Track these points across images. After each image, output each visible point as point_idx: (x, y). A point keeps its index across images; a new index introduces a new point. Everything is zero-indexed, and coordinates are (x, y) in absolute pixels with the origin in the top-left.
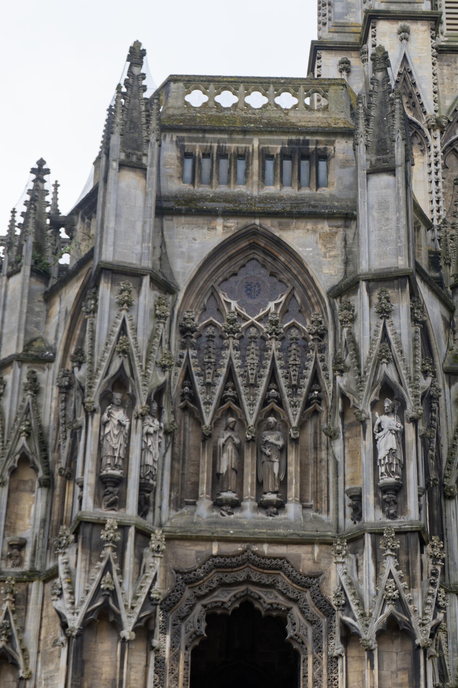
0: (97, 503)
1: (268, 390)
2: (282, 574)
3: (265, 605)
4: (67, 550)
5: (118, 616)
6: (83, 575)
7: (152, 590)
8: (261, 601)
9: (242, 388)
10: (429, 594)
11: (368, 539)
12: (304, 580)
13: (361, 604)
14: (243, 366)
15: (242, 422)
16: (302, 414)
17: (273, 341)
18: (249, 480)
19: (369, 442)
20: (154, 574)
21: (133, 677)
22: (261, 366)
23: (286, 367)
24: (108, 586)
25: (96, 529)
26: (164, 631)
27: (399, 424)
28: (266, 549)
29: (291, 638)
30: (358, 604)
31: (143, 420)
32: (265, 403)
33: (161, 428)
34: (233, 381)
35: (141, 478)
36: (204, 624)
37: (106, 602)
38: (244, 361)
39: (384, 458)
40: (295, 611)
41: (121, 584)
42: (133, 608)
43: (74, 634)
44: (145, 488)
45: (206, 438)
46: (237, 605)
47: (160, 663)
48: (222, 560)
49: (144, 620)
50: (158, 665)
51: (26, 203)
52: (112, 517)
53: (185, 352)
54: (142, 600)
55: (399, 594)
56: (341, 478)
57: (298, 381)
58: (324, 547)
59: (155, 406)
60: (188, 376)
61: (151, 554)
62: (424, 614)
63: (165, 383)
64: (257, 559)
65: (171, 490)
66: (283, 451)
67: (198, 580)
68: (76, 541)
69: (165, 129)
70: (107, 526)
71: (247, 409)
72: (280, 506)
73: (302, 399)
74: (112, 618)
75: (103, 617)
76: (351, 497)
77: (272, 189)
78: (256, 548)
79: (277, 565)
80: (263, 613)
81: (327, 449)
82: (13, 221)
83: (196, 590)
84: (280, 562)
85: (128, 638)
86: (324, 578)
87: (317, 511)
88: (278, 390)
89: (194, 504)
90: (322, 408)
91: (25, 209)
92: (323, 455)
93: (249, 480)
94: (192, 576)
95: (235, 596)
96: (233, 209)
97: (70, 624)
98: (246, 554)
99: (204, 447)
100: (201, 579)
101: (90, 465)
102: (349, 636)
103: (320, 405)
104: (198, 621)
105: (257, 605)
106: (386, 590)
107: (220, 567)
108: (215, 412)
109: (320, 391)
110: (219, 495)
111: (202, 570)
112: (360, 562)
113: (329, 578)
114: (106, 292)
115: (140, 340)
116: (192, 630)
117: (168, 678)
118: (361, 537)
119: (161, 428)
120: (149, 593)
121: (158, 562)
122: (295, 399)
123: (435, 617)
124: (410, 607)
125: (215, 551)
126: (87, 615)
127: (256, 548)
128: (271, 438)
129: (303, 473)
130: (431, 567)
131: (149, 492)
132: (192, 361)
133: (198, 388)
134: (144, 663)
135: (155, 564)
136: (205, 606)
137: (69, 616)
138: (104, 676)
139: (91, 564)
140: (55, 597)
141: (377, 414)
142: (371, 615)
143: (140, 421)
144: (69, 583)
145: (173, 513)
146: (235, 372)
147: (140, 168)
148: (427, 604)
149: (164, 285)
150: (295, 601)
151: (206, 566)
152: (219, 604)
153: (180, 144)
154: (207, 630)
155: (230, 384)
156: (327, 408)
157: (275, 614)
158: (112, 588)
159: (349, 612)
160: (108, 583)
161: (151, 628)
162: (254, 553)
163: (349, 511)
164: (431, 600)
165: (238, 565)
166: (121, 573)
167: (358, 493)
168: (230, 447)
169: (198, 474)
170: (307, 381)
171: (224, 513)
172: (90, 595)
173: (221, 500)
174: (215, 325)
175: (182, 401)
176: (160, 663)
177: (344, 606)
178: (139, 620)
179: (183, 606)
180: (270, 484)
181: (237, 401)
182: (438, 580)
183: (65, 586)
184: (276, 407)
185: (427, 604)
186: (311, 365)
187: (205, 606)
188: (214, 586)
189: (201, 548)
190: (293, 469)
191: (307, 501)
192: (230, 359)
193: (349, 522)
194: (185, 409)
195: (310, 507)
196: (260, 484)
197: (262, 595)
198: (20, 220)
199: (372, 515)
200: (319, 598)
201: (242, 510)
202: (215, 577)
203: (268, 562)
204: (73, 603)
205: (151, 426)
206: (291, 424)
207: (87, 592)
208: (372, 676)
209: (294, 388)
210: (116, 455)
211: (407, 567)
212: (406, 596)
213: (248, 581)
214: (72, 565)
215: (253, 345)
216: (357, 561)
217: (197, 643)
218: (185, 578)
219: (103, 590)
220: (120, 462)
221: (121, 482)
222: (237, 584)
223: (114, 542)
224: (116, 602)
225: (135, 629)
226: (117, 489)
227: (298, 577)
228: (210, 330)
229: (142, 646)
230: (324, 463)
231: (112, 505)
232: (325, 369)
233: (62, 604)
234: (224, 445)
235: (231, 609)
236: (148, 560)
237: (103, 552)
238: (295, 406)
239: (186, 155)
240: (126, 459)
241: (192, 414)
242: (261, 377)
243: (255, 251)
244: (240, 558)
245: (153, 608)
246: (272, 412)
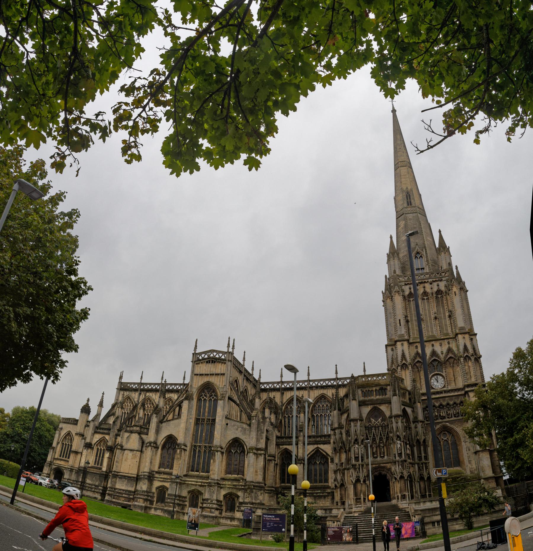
44: (362, 457)
52: (357, 463)
60: (367, 435)
69: (358, 388)
75: (358, 480)
77: (378, 397)
96: (372, 402)
101: (353, 455)
114: (352, 424)
115: (358, 432)
128: (381, 445)
147: (355, 400)
149: (361, 420)
153: (361, 390)
176: (367, 486)
221: (358, 457)
233: (351, 478)
239: (362, 391)
240: (358, 454)
243: (376, 412)
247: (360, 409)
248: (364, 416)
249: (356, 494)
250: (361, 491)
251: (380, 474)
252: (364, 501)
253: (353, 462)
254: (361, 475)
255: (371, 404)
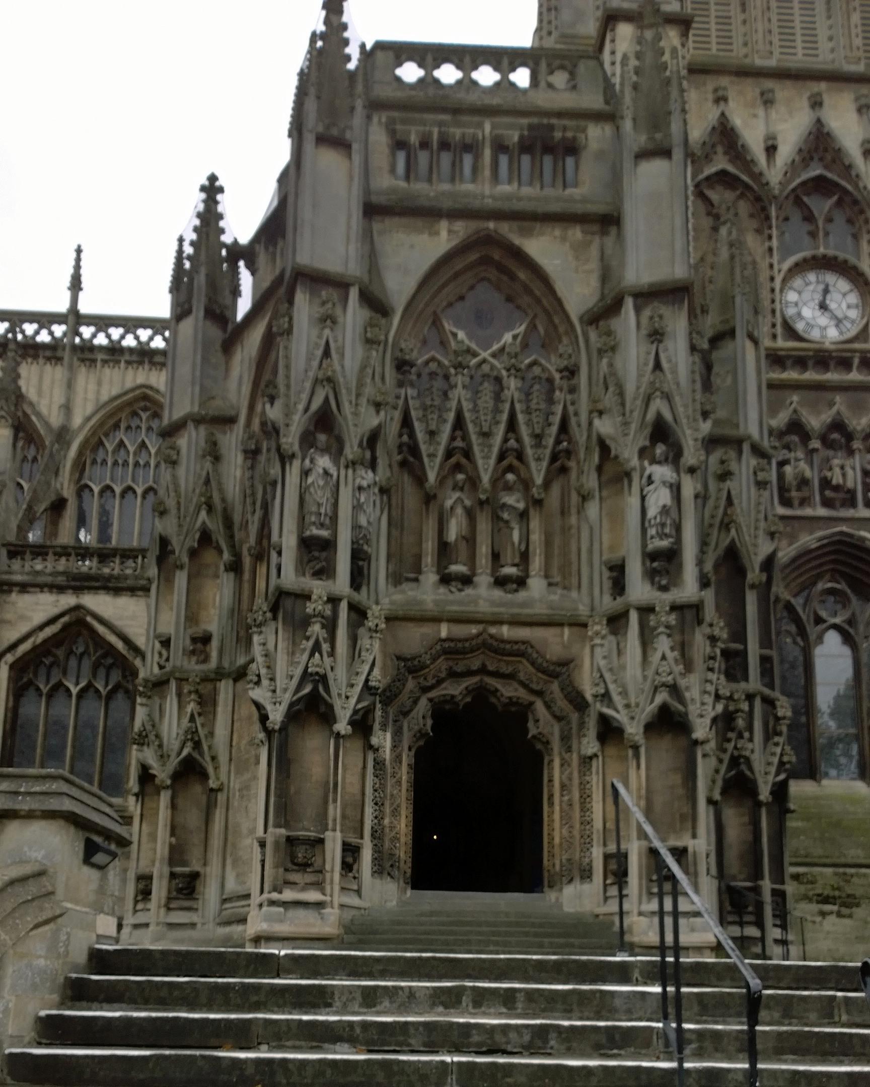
0: (300, 569)
1: (506, 440)
2: (524, 661)
3: (502, 699)
4: (263, 629)
5: (331, 707)
6: (286, 657)
7: (371, 678)
8: (499, 694)
9: (474, 437)
10: (707, 681)
11: (634, 616)
12: (552, 668)
13: (624, 693)
14: (475, 410)
15: (473, 482)
16: (548, 471)
17: (512, 379)
18: (484, 550)
19: (634, 501)
20: (372, 658)
21: (348, 781)
22: (497, 411)
23: (528, 411)
24: (318, 669)
25: (299, 602)
26: (384, 727)
27: (675, 475)
28: (505, 631)
29: (534, 737)
30: (620, 693)
31: (354, 471)
32: (502, 457)
33: (375, 483)
34: (461, 429)
35: (353, 543)
36: (429, 722)
37: (315, 690)
38: (476, 405)
39: (655, 518)
40: (539, 706)
41: (332, 668)
42: (347, 697)
43: (277, 727)
44: (359, 556)
45: (429, 499)
46: (468, 699)
47: (379, 764)
48: (452, 645)
49: (361, 713)
50: (378, 767)
51: (196, 229)
52: (319, 588)
53: (403, 391)
54: (358, 689)
55: (674, 679)
56: (596, 546)
57: (543, 430)
58: (576, 629)
59: (368, 455)
60: (406, 422)
61: (368, 635)
62: (703, 704)
63: (380, 426)
64: (495, 644)
65: (388, 561)
66: (524, 516)
67: (422, 668)
68: (275, 618)
70: (314, 597)
71: (480, 462)
72: (521, 582)
73: (548, 452)
74: (323, 709)
75: (312, 707)
76: (611, 569)
78: (493, 630)
79: (520, 651)
80: (500, 708)
81: (579, 512)
82: (180, 251)
83: (421, 680)
84: (523, 647)
85: (343, 732)
86: (576, 666)
87: (565, 588)
88: (519, 440)
89: (416, 580)
90: (572, 464)
91: (194, 236)
92: (573, 520)
93: (484, 550)
94: (416, 662)
95: (466, 688)
97: (271, 717)
98: (481, 638)
99: (427, 510)
100: (428, 667)
102: (609, 732)
103: (569, 459)
104: (424, 717)
105: (493, 700)
106: (657, 673)
107: (450, 653)
108: (441, 467)
109: (569, 443)
110: (446, 568)
111: (428, 656)
112: (622, 645)
113: (582, 666)
116: (416, 728)
117: (390, 782)
118: (625, 614)
119: (375, 483)
120: (367, 681)
121: (377, 645)
122: (540, 451)
123: (714, 708)
124: (687, 695)
125: (444, 634)
126: (292, 705)
127: (493, 630)
129: (548, 543)
130: (708, 649)
131: (364, 560)
132: (411, 402)
133: (420, 436)
134: (361, 765)
135: (372, 648)
136: (431, 700)
137: (269, 707)
138: (314, 779)
139: (294, 643)
140: (251, 685)
141: (646, 463)
142: (637, 705)
143: (350, 471)
144: (268, 667)
145: (391, 589)
146: (464, 418)
148: (705, 692)
150: (539, 693)
151: (433, 651)
152: (448, 698)
154: (433, 728)
155: (459, 433)
156: (578, 463)
157: (513, 709)
158: (321, 671)
159: (610, 703)
160: (317, 666)
161: (370, 723)
162: (491, 636)
163: (607, 584)
164: (710, 688)
165: (472, 651)
166: (332, 654)
167: (620, 563)
168: (459, 511)
169: (420, 544)
170: (554, 429)
171: (453, 589)
172: (295, 681)
173: (450, 574)
174: (439, 363)
175: (399, 453)
176: (379, 764)
177: (603, 696)
178: (355, 712)
179: (404, 698)
180: (508, 556)
181: (468, 454)
182: (717, 665)
183: (263, 671)
184: (516, 463)
185: (705, 692)
186: (559, 409)
187: (431, 700)
188: (443, 675)
189: (427, 629)
190: (536, 537)
191: (552, 577)
192: (459, 401)
193: (607, 598)
194: (403, 464)
195: (556, 584)
196: (496, 557)
197: (499, 687)
198: (188, 250)
199: (639, 589)
200: (570, 689)
201: (475, 587)
202: (442, 665)
203: (508, 646)
204: (274, 691)
205: (363, 478)
206: (533, 483)
207: (292, 677)
208: (639, 777)
209: (538, 438)
210: (323, 511)
211: (683, 648)
212: (682, 683)
213: (483, 670)
214: (271, 646)
215: (486, 384)
216: (618, 644)
217: (421, 743)
218: (408, 666)
219: (311, 674)
220: (327, 521)
221: (328, 545)
222: (470, 673)
223: (323, 617)
224: (327, 689)
225: (352, 723)
226: (324, 554)
227: (545, 665)
228: (433, 366)
229: (357, 745)
230: (574, 531)
231: (319, 574)
232: (576, 414)
234: (452, 508)
235: (462, 704)
236: (364, 641)
237: (310, 629)
238: (538, 459)
240: (334, 518)
241: (411, 472)
242: (498, 423)
244: (474, 642)
245: (372, 698)
246: (510, 469)
247: (368, 236)
248: (399, 286)
249: (283, 807)
250: (329, 789)
251: (481, 694)
252: (347, 867)
253: (290, 576)
254: (339, 678)
255: (454, 215)
